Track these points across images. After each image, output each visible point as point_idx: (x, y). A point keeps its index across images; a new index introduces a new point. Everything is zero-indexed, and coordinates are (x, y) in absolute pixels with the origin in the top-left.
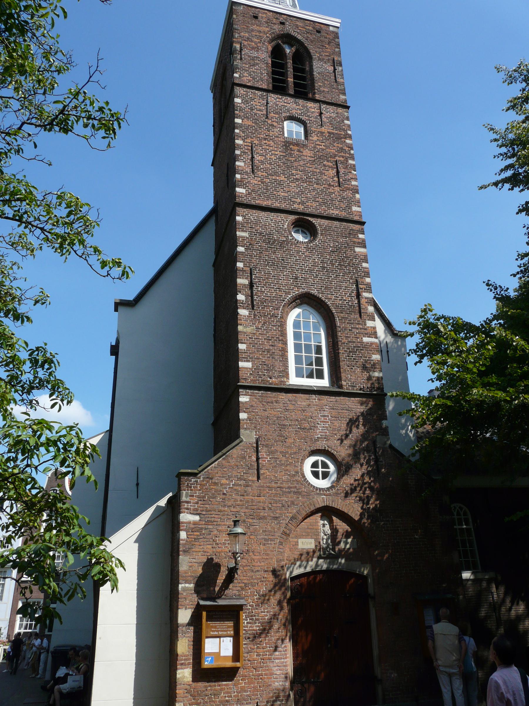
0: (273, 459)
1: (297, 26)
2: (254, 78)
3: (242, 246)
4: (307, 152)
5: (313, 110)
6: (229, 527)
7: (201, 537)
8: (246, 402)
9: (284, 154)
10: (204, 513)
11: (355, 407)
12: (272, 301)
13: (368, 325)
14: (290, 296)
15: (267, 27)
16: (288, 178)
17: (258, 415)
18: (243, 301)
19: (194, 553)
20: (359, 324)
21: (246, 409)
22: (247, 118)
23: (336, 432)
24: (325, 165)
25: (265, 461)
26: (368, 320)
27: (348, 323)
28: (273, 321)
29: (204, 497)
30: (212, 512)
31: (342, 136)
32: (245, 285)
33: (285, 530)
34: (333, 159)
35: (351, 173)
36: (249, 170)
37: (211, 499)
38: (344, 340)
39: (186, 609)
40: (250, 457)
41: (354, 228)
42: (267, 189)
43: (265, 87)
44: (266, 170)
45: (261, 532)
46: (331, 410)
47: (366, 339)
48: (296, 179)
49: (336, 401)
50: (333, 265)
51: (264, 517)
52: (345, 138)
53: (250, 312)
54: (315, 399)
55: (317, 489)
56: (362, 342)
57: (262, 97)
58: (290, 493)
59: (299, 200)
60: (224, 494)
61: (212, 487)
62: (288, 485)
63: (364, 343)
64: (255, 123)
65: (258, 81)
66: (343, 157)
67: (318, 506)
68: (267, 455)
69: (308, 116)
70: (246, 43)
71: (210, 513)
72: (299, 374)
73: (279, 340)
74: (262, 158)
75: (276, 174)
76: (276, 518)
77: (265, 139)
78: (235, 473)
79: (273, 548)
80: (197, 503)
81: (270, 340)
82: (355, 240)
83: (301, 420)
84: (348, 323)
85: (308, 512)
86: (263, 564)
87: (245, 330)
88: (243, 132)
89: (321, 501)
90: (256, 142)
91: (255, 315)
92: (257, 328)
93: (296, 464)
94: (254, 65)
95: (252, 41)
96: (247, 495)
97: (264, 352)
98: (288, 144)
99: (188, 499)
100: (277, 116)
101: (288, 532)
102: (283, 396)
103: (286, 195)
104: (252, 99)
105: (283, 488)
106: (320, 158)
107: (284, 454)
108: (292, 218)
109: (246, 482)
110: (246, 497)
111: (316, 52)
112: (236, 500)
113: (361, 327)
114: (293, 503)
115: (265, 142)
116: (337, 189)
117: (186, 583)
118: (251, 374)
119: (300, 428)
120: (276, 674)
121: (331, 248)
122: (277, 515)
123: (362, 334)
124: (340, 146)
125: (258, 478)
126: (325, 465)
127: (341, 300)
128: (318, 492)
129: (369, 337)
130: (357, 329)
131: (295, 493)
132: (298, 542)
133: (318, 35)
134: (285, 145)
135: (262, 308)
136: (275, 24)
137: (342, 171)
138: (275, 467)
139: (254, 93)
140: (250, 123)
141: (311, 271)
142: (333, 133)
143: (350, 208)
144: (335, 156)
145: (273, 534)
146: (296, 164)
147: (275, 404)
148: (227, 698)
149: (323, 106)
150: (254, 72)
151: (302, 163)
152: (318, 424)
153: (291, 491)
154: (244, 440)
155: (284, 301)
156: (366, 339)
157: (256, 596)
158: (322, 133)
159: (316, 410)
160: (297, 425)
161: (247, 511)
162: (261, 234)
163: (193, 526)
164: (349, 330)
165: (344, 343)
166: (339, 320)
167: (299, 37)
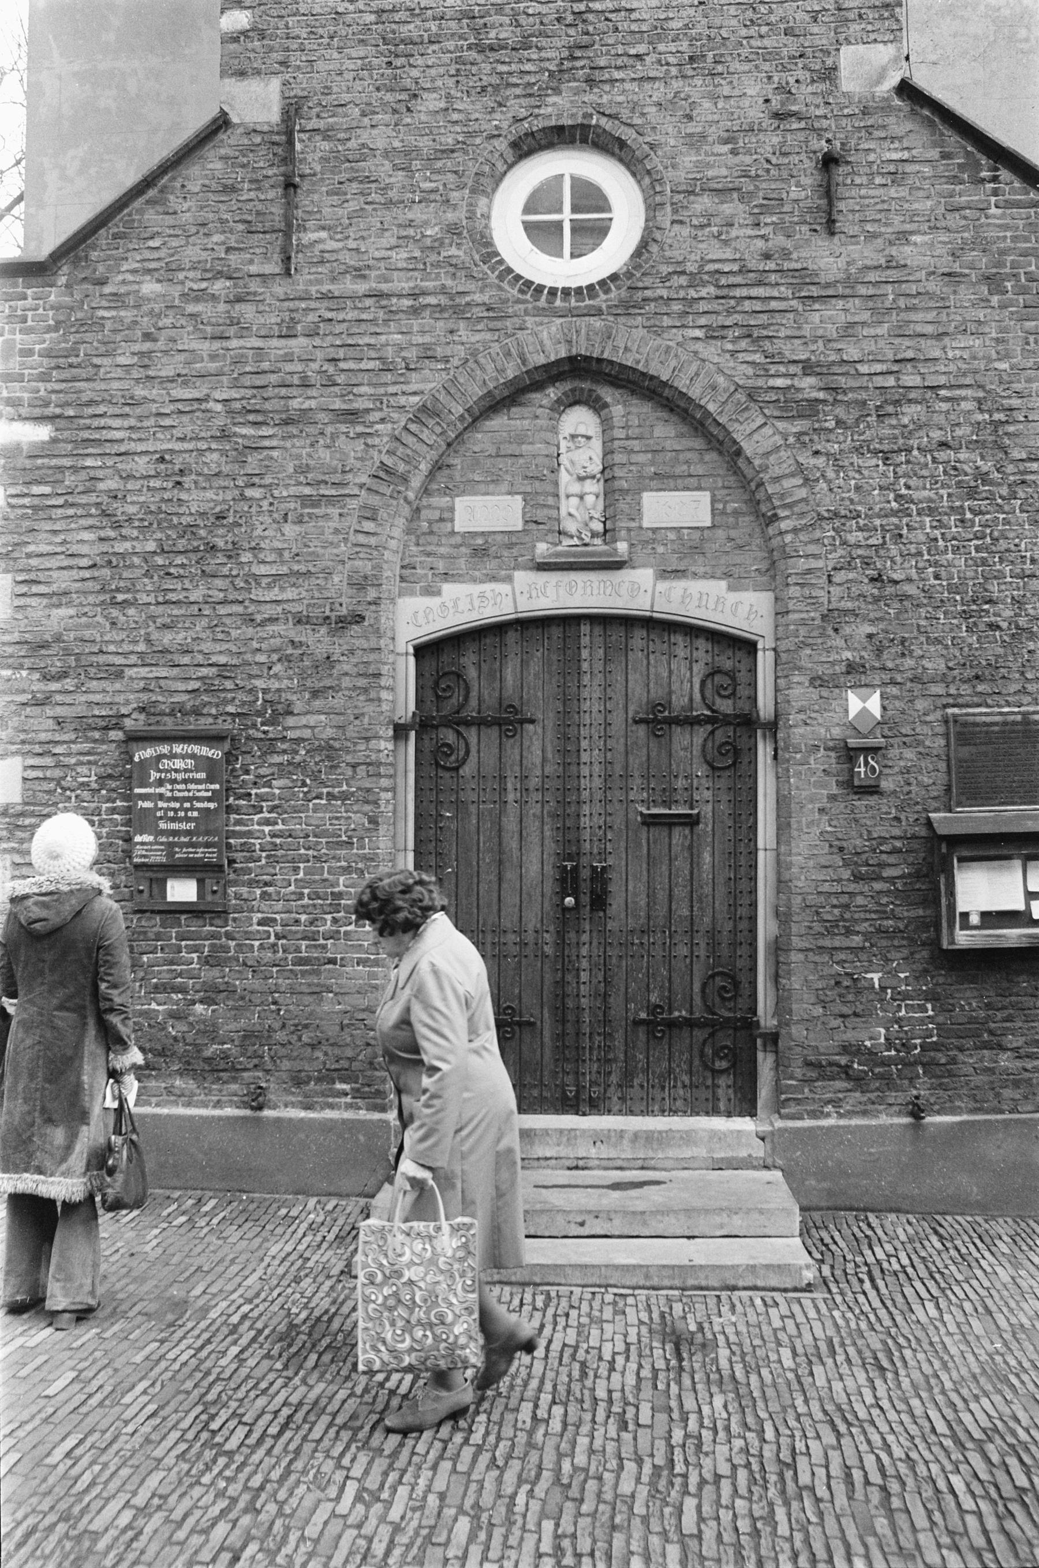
0: (355, 185)
6: (162, 460)
23: (641, 49)
30: (101, 409)
33: (389, 461)
37: (96, 361)
62: (412, 284)
76: (352, 416)
78: (193, 253)
79: (337, 531)
85: (491, 385)
101: (402, 467)
109: (235, 286)
110: (234, 343)
114: (428, 355)
119: (480, 48)
122: (360, 404)
128: (542, 302)
132: (452, 509)
145: (337, 478)
161: (234, 394)
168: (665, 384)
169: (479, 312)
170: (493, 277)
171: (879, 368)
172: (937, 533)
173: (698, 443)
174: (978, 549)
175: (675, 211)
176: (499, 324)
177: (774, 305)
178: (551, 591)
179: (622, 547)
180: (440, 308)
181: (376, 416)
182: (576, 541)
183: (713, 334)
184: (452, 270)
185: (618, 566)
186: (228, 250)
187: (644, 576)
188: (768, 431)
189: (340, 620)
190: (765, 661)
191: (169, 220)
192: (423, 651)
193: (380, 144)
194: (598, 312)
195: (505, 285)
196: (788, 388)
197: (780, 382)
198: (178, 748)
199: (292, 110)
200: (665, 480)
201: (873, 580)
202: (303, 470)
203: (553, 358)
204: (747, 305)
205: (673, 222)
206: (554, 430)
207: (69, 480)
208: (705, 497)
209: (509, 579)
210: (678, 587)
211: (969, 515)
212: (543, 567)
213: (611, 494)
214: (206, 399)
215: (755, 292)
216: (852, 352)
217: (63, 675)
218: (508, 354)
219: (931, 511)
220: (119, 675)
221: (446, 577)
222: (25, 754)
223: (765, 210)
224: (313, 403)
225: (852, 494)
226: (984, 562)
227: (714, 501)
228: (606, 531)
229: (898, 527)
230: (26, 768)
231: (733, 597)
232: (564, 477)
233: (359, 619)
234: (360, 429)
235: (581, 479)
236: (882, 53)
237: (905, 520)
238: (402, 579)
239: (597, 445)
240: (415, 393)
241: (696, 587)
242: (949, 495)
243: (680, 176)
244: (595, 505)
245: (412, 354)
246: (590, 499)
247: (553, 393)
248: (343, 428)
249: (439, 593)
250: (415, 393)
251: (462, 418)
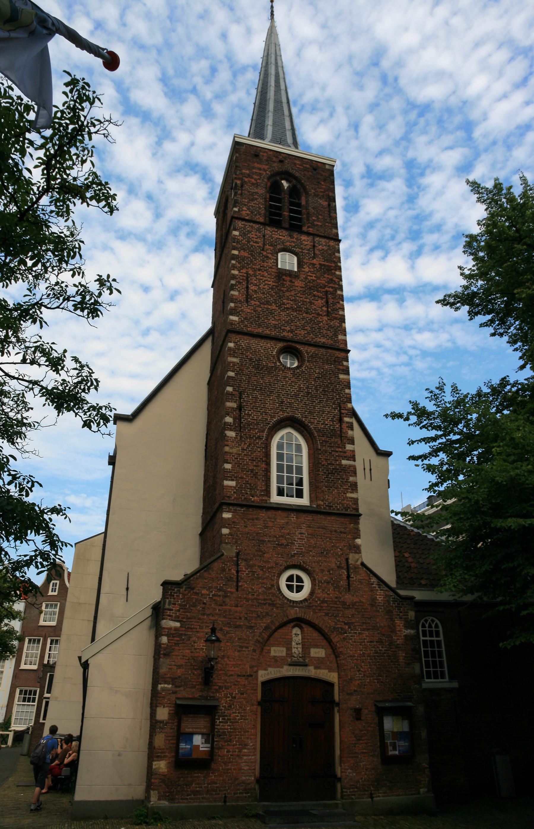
1: (295, 164)
2: (252, 212)
3: (232, 371)
4: (298, 283)
5: (306, 243)
7: (181, 642)
8: (229, 518)
9: (276, 284)
10: (184, 620)
11: (330, 526)
12: (257, 424)
13: (347, 448)
14: (275, 420)
15: (267, 165)
16: (280, 307)
17: (239, 531)
18: (231, 423)
19: (174, 657)
20: (339, 447)
21: (228, 525)
22: (244, 250)
24: (314, 296)
25: (243, 574)
26: (348, 444)
27: (328, 446)
28: (258, 443)
29: (186, 605)
30: (192, 620)
31: (332, 268)
32: (233, 408)
33: (259, 638)
34: (323, 290)
35: (339, 303)
36: (242, 298)
37: (192, 608)
38: (324, 462)
39: (164, 707)
40: (230, 570)
41: (339, 356)
42: (258, 317)
43: (262, 220)
44: (259, 299)
45: (237, 639)
46: (308, 528)
47: (344, 462)
48: (287, 308)
49: (313, 520)
50: (317, 390)
51: (240, 625)
52: (336, 270)
53: (236, 433)
54: (293, 517)
55: (291, 601)
56: (340, 465)
57: (259, 230)
58: (265, 604)
59: (288, 328)
60: (204, 603)
61: (193, 596)
63: (342, 465)
64: (252, 255)
65: (256, 215)
66: (332, 287)
67: (290, 617)
68: (246, 569)
69: (302, 248)
70: (246, 180)
71: (190, 620)
72: (280, 492)
73: (263, 461)
74: (256, 288)
75: (268, 303)
76: (251, 627)
77: (259, 270)
78: (215, 584)
79: (247, 654)
80: (179, 611)
81: (254, 460)
82: (341, 367)
83: (279, 537)
84: (328, 446)
86: (236, 669)
87: (231, 451)
88: (240, 263)
89: (294, 613)
90: (251, 272)
91: (241, 437)
92: (243, 449)
93: (273, 578)
94: (253, 200)
95: (252, 178)
96: (226, 605)
97: (248, 471)
98: (282, 274)
99: (171, 607)
100: (272, 248)
102: (263, 514)
103: (277, 323)
104: (249, 232)
105: (259, 600)
106: (310, 288)
107: (262, 568)
108: (281, 345)
110: (224, 607)
111: (312, 188)
112: (215, 609)
113: (340, 450)
114: (267, 614)
115: (259, 272)
116: (325, 318)
117: (165, 684)
118: (234, 492)
120: (244, 769)
121: (316, 375)
122: (253, 625)
123: (342, 456)
124: (330, 277)
125: (237, 590)
126: (299, 579)
127: (322, 424)
128: (291, 604)
129: (348, 460)
130: (337, 452)
131: (269, 604)
132: (270, 650)
133: (315, 172)
134: (278, 276)
135: (248, 430)
136: (274, 162)
137: (331, 301)
138: (253, 579)
139: (252, 227)
140: (246, 255)
141: (296, 395)
142: (324, 265)
143: (336, 336)
144: (325, 286)
146: (287, 294)
147: (255, 521)
148: (198, 789)
149: (317, 239)
150: (252, 206)
151: (293, 293)
152: (295, 541)
153: (266, 603)
154: (225, 554)
155: (269, 424)
156: (344, 462)
157: (229, 697)
158: (314, 265)
159: (294, 528)
160: (275, 542)
161: (224, 619)
162: (251, 359)
163: (175, 632)
164: (330, 453)
165: (323, 465)
166: (320, 443)
167: (297, 174)
168: (316, 625)
169: (278, 605)
170: (281, 597)
173: (322, 638)
180: (269, 604)
181: (256, 628)
183: (327, 614)
185: (306, 665)
187: (311, 668)
188: (337, 637)
189: (248, 676)
190: (336, 688)
191: (210, 576)
192: (263, 683)
199: (238, 554)
200: (316, 646)
206: (291, 632)
210: (318, 671)
212: (290, 665)
216: (353, 620)
217: (179, 687)
219: (369, 656)
221: (270, 666)
222: (169, 707)
230: (170, 710)
231: (329, 674)
232: (293, 643)
233: (251, 676)
235: (297, 644)
236: (357, 556)
239: (300, 637)
241: (322, 671)
245: (264, 614)
246: (299, 649)
247: (292, 624)
249: (267, 670)
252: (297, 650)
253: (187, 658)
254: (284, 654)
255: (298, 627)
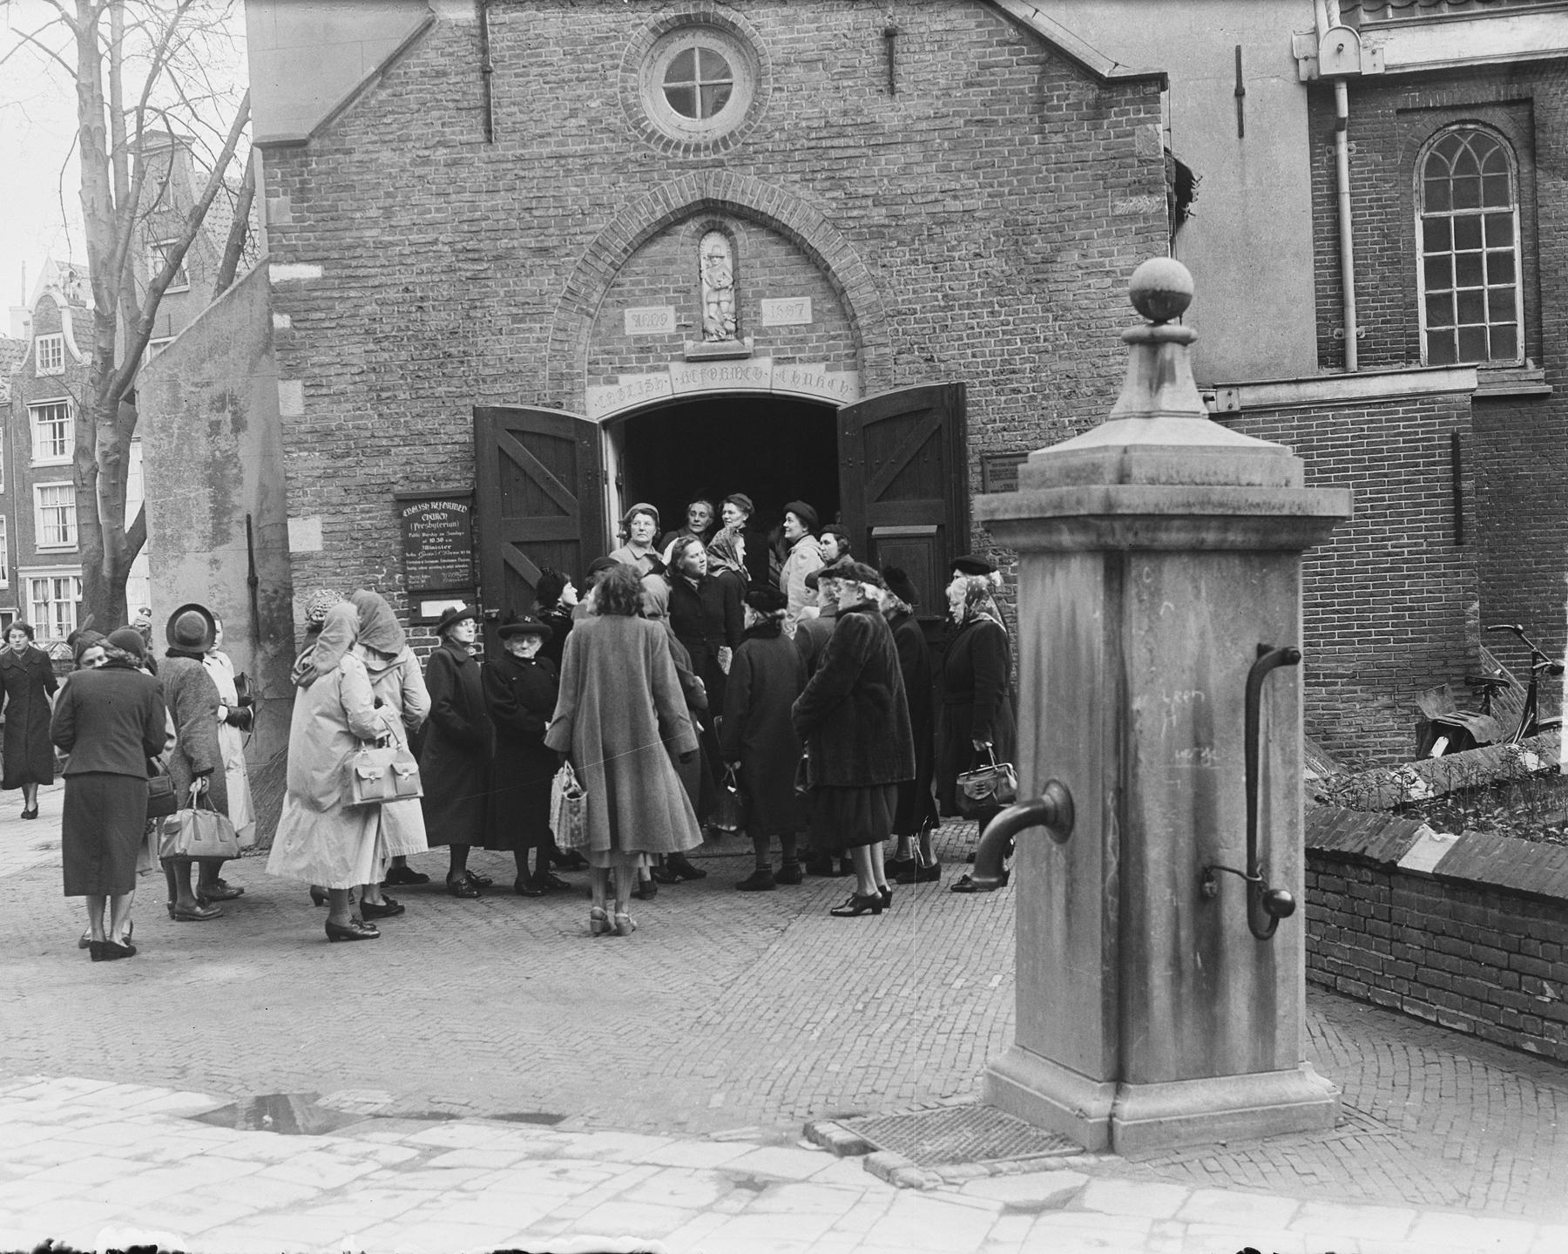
6: (407, 290)
30: (359, 252)
62: (583, 147)
76: (543, 251)
79: (539, 340)
132: (622, 320)
145: (536, 299)
168: (772, 218)
171: (931, 197)
172: (974, 322)
174: (1004, 333)
175: (776, 80)
176: (647, 176)
177: (850, 152)
178: (698, 377)
179: (748, 341)
182: (715, 338)
184: (612, 135)
186: (443, 125)
187: (765, 363)
193: (552, 32)
194: (721, 164)
195: (652, 146)
196: (863, 217)
197: (855, 213)
198: (435, 505)
200: (777, 290)
201: (927, 360)
202: (515, 294)
203: (690, 201)
204: (833, 154)
205: (775, 89)
207: (339, 307)
208: (807, 301)
209: (666, 368)
210: (789, 369)
211: (997, 307)
212: (690, 360)
213: (739, 301)
214: (435, 242)
215: (836, 142)
216: (910, 186)
218: (656, 200)
220: (388, 453)
221: (622, 370)
223: (843, 75)
224: (516, 243)
225: (911, 296)
226: (1009, 342)
227: (813, 302)
228: (737, 329)
229: (944, 320)
231: (829, 376)
232: (706, 288)
234: (551, 262)
237: (949, 314)
238: (590, 372)
240: (589, 233)
241: (801, 369)
242: (982, 293)
243: (779, 52)
244: (728, 307)
246: (724, 305)
247: (693, 225)
248: (538, 261)
249: (616, 382)
250: (589, 233)
251: (625, 251)
252: (717, 310)
253: (355, 370)
254: (671, 327)
255: (719, 230)
